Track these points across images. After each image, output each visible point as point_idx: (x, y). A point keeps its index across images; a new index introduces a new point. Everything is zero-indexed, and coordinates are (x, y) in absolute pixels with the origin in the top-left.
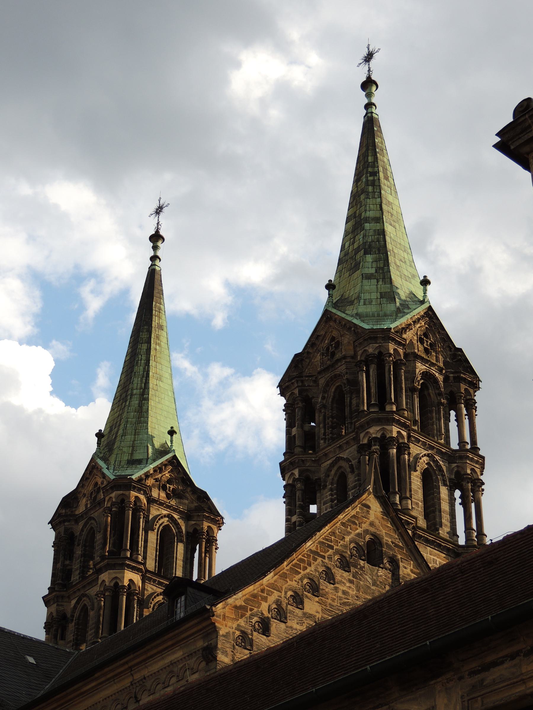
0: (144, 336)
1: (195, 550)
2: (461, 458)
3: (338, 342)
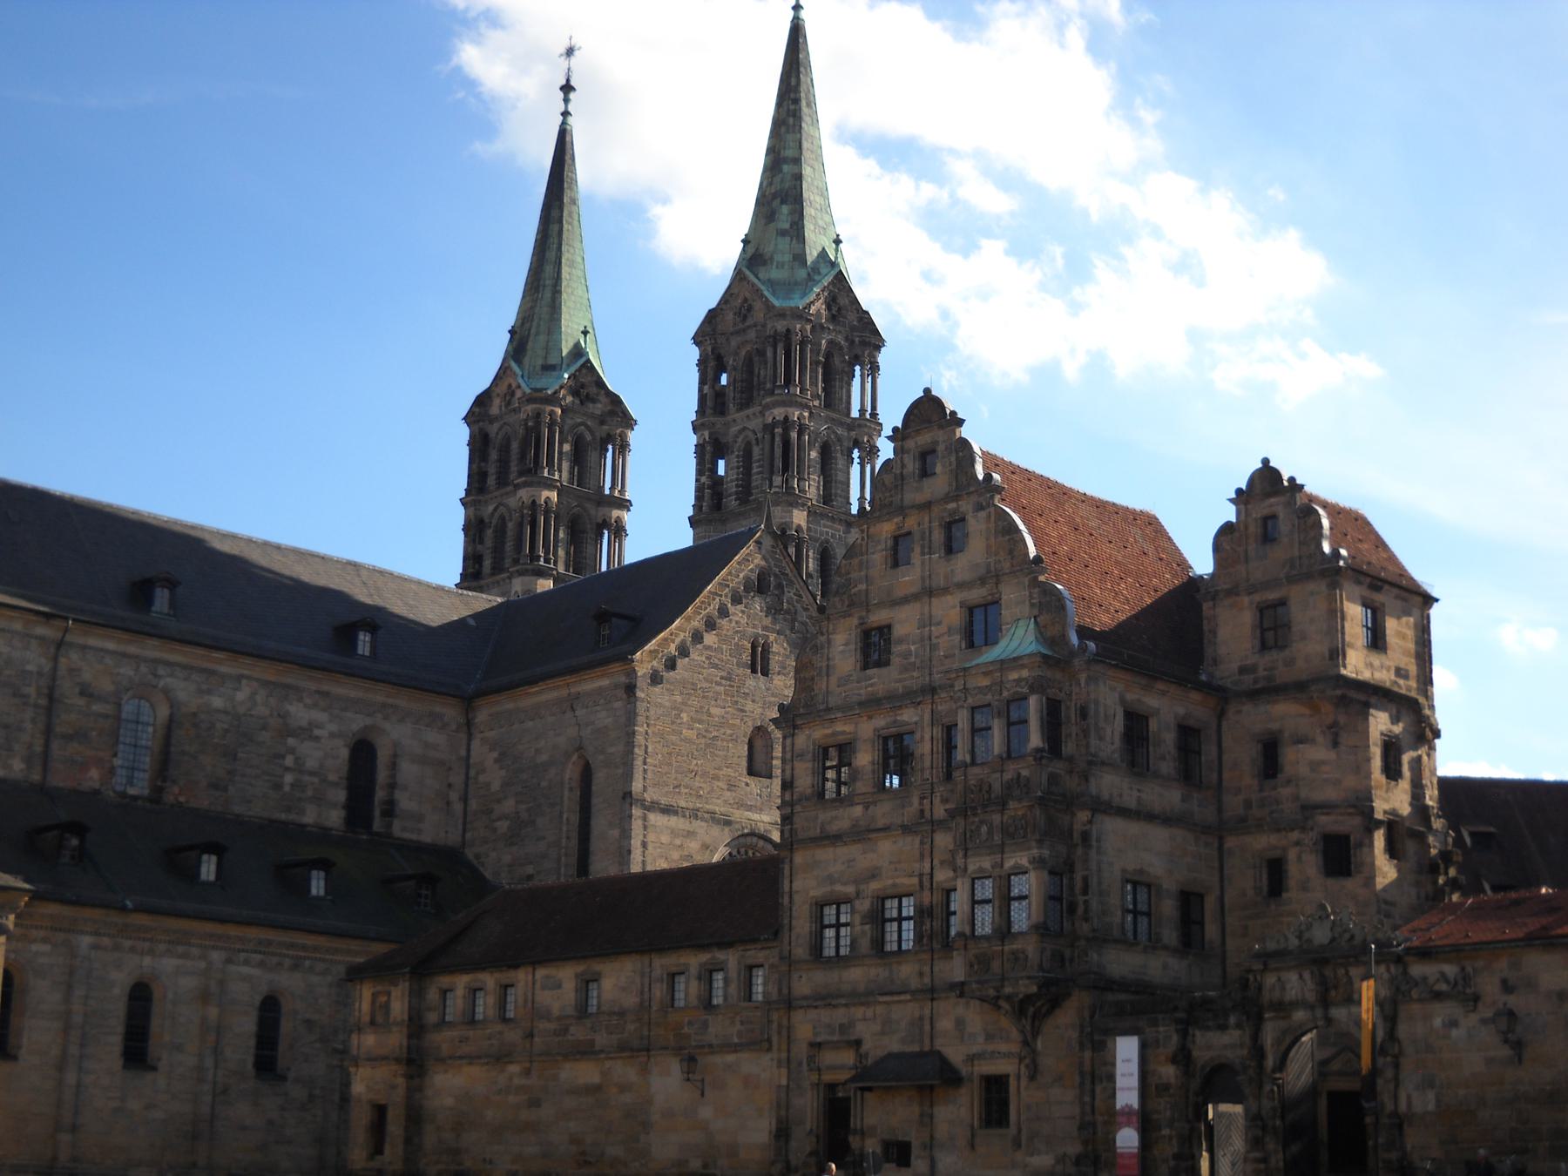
0: (555, 213)
1: (607, 450)
2: (860, 426)
3: (750, 305)
